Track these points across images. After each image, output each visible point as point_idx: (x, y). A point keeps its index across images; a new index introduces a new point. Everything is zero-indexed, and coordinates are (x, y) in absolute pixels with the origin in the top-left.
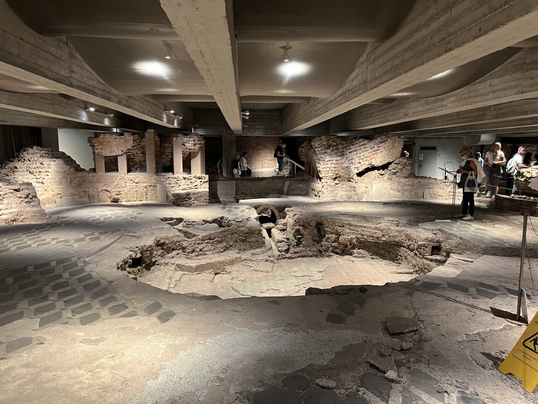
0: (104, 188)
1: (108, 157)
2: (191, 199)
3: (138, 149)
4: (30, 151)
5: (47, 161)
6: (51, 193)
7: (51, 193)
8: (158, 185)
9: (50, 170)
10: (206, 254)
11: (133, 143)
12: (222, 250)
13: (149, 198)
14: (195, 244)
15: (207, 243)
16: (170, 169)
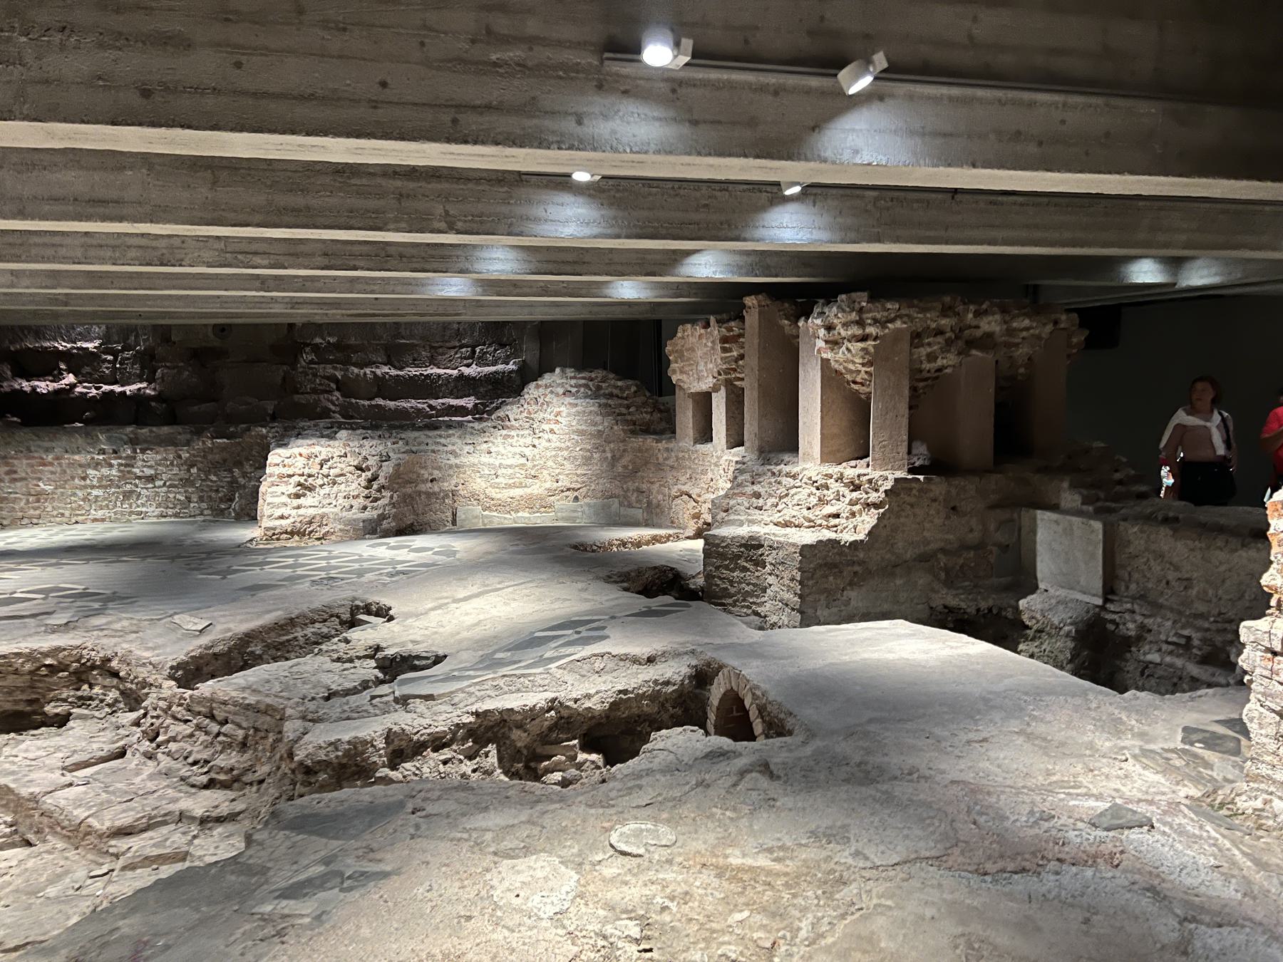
0: (685, 488)
4: (547, 378)
6: (548, 485)
14: (165, 711)
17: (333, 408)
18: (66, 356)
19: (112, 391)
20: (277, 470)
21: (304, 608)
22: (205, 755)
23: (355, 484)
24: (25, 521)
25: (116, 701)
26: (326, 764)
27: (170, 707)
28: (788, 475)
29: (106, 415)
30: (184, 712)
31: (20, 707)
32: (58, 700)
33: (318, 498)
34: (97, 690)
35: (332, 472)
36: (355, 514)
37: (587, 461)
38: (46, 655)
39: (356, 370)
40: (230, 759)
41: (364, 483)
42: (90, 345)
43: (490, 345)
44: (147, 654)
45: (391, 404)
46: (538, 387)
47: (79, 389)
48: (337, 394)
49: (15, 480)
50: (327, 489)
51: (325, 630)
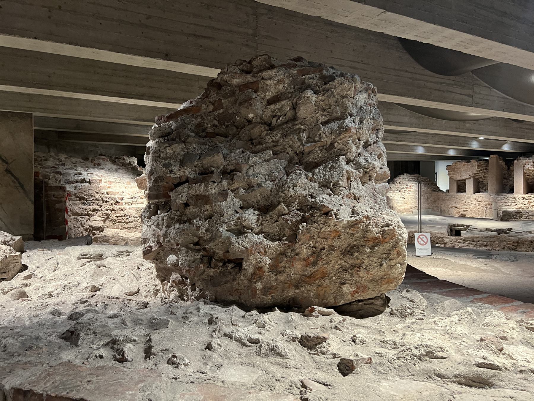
0: (454, 205)
1: (459, 180)
2: (522, 217)
3: (485, 173)
4: (402, 176)
5: (410, 184)
6: (410, 205)
7: (410, 205)
8: (493, 204)
9: (411, 190)
11: (478, 168)
13: (488, 215)
15: (469, 243)
16: (512, 191)
28: (512, 198)
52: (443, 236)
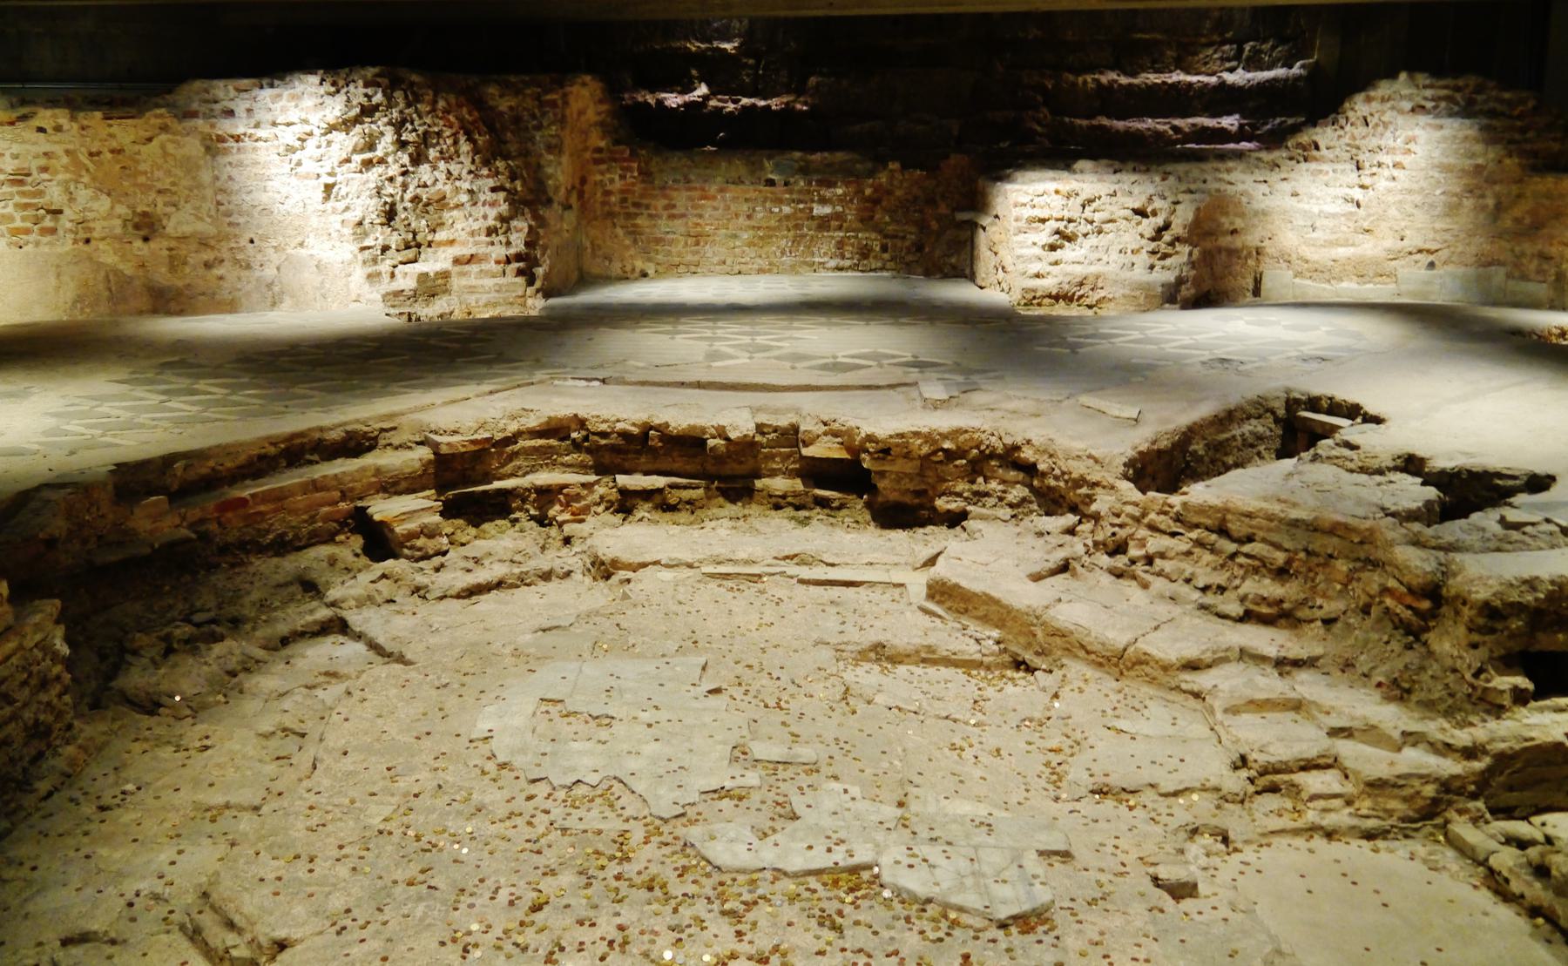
4: (1384, 88)
6: (1390, 242)
9: (1406, 160)
10: (1145, 586)
12: (1235, 609)
14: (1137, 520)
15: (1199, 543)
17: (1039, 129)
18: (698, 59)
19: (754, 105)
20: (1016, 212)
21: (1233, 401)
22: (1220, 578)
23: (1134, 235)
24: (682, 269)
25: (1024, 500)
26: (1519, 608)
27: (1144, 515)
29: (748, 140)
30: (1171, 523)
31: (908, 499)
32: (951, 494)
33: (1083, 251)
34: (993, 485)
35: (1097, 217)
36: (1140, 274)
37: (1452, 210)
38: (945, 437)
39: (1071, 77)
40: (1270, 588)
41: (1149, 232)
42: (727, 46)
43: (1265, 41)
44: (1078, 446)
45: (1120, 125)
46: (1369, 100)
47: (713, 103)
48: (1045, 110)
49: (672, 217)
50: (1093, 240)
51: (1260, 429)
52: (1093, 478)
